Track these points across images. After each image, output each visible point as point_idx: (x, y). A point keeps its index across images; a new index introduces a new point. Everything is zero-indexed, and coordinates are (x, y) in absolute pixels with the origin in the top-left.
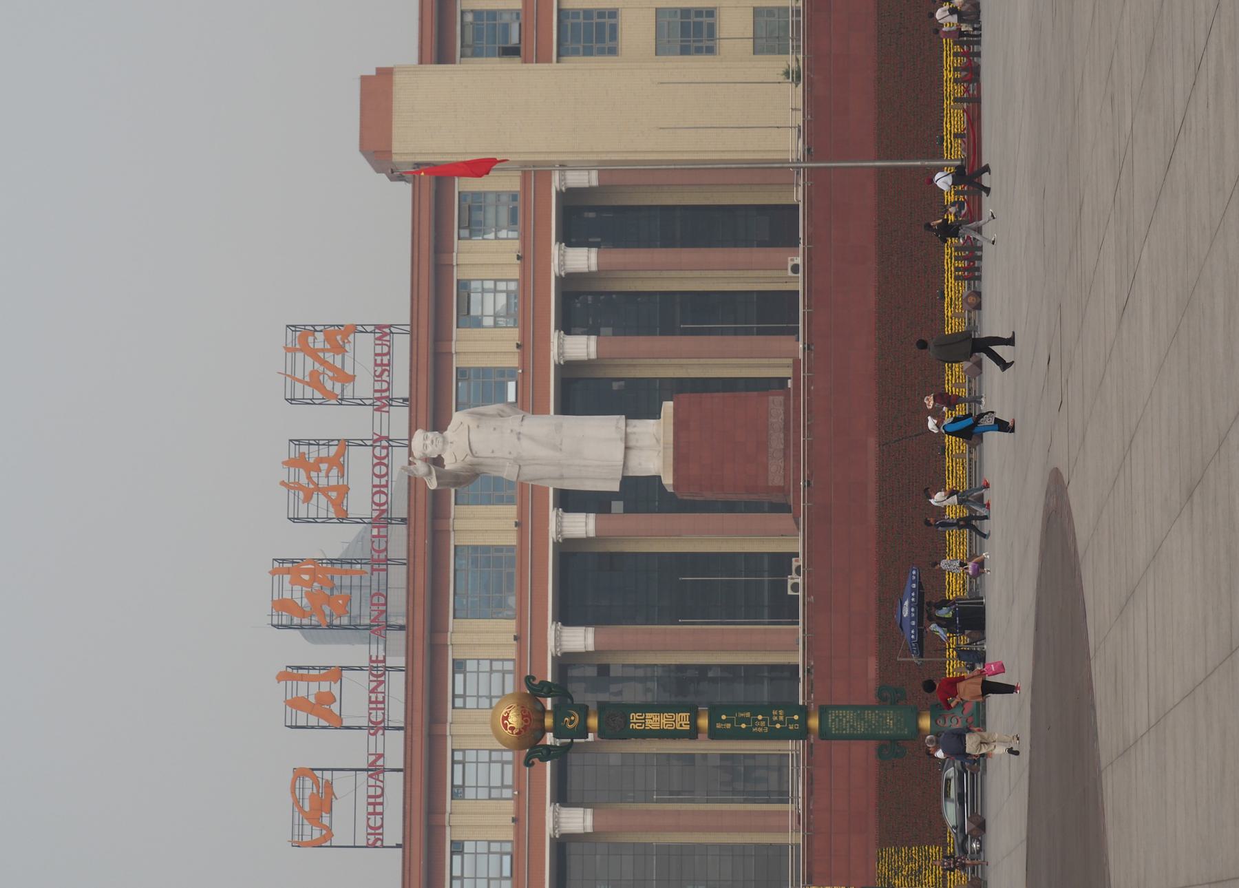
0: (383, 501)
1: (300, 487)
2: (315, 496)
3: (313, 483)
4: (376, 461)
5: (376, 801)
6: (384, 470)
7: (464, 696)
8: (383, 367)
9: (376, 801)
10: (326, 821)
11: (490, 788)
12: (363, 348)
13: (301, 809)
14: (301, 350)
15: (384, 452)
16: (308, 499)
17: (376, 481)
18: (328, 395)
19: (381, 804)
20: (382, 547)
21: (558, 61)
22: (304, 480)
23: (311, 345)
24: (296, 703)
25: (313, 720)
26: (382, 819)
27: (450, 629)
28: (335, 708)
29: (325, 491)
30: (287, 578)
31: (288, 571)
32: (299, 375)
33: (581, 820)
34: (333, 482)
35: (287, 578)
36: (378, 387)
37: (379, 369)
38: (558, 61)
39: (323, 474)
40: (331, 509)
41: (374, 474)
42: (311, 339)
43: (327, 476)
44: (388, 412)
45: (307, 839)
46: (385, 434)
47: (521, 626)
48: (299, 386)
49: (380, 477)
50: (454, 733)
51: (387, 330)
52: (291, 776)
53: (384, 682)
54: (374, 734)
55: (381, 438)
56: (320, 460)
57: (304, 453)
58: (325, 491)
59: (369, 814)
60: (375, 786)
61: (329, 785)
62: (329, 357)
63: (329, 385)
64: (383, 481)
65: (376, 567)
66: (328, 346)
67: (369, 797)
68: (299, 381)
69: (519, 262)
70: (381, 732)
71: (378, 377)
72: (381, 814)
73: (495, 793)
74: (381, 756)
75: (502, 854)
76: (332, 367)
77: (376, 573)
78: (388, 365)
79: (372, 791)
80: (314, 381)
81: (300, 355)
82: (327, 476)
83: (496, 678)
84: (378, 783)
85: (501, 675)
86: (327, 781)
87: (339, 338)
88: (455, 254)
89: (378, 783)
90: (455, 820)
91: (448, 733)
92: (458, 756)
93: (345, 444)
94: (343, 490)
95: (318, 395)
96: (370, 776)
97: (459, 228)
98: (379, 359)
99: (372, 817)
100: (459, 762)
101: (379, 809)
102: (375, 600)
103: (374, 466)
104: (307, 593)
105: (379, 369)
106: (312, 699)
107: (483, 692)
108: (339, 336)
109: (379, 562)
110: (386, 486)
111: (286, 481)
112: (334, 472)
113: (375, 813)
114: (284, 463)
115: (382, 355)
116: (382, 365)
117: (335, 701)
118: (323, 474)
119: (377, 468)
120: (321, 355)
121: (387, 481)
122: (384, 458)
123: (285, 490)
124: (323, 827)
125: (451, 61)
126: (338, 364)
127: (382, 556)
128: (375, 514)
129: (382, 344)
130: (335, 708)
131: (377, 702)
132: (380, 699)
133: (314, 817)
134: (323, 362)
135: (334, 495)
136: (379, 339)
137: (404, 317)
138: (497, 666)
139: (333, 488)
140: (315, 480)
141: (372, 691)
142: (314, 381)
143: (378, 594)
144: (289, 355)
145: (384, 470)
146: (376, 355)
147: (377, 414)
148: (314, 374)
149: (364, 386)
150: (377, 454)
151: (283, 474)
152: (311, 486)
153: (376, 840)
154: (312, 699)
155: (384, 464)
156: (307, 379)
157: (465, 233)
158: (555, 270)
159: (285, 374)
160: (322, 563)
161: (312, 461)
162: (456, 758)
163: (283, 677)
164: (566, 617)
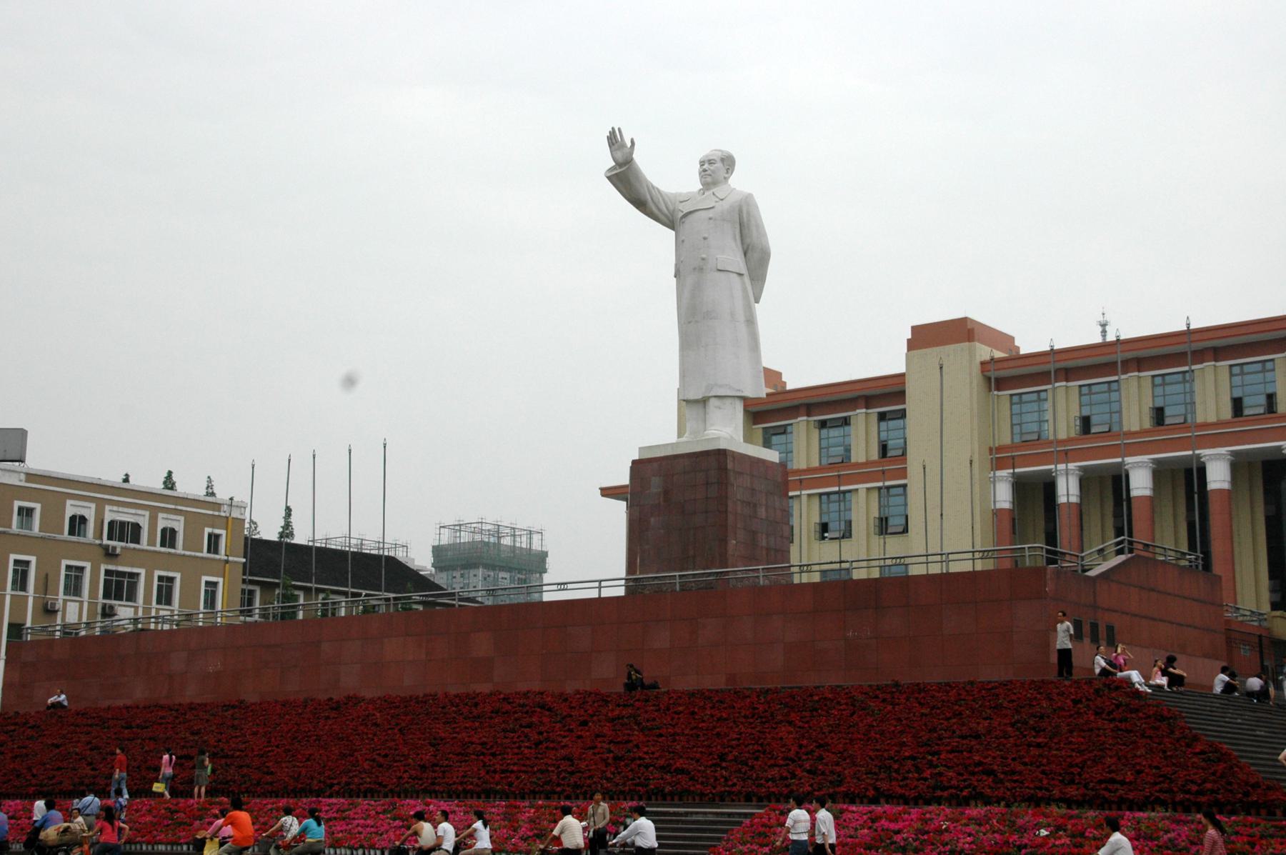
7: (1242, 373)
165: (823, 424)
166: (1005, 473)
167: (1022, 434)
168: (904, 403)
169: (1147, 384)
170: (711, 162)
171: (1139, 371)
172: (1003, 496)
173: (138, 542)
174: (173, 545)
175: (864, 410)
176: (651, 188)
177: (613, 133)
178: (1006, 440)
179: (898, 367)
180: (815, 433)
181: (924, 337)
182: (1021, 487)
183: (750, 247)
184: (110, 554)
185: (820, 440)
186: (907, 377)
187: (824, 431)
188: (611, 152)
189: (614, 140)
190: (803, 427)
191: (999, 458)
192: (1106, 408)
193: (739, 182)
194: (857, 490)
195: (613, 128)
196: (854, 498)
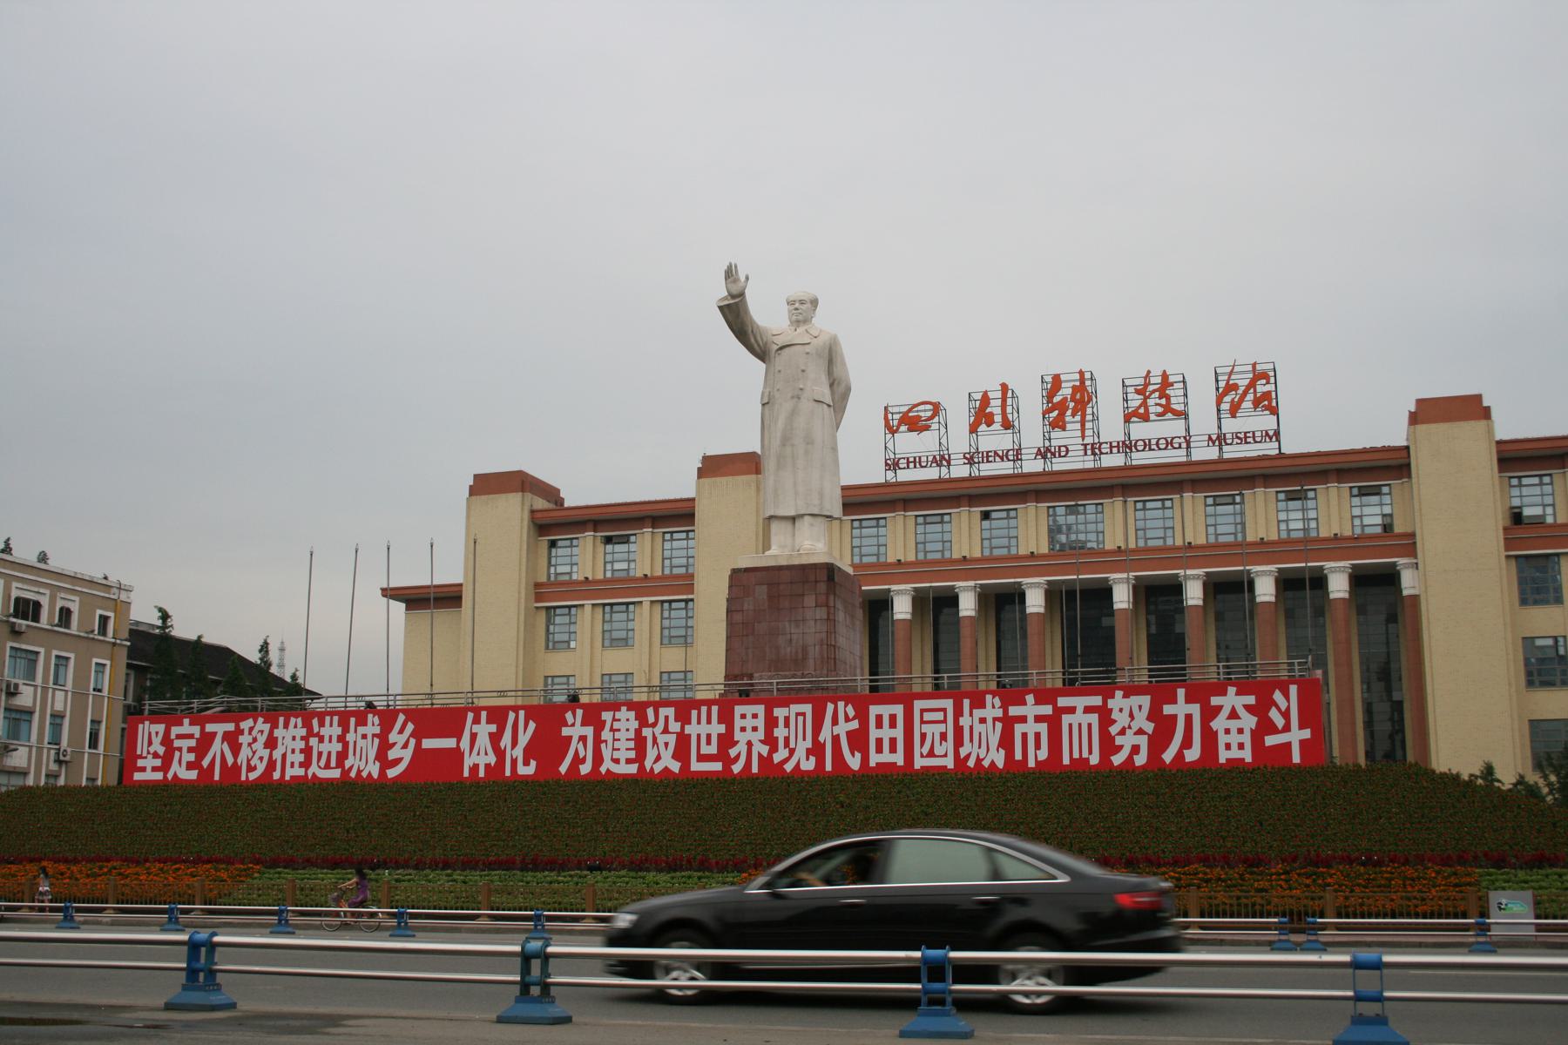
0: (1138, 448)
1: (1146, 385)
2: (1142, 397)
3: (1150, 395)
4: (1169, 440)
5: (916, 462)
6: (1162, 446)
8: (1244, 438)
9: (916, 462)
10: (903, 428)
11: (924, 543)
12: (1266, 422)
13: (910, 410)
14: (1254, 375)
16: (1138, 392)
17: (1154, 442)
18: (1219, 402)
19: (915, 467)
20: (1103, 451)
21: (1508, 557)
22: (1151, 388)
23: (1259, 382)
24: (985, 400)
26: (904, 468)
27: (1039, 505)
28: (983, 427)
29: (1144, 404)
30: (1078, 383)
32: (1233, 377)
33: (1034, 604)
34: (1152, 409)
35: (1078, 383)
36: (1228, 436)
37: (1242, 436)
38: (1508, 557)
39: (1158, 401)
40: (1130, 410)
41: (1159, 439)
42: (1264, 381)
43: (1157, 404)
44: (1208, 446)
45: (890, 416)
46: (1192, 445)
48: (1226, 378)
49: (1157, 444)
50: (963, 514)
51: (1274, 439)
52: (934, 401)
53: (1003, 460)
54: (965, 458)
55: (1188, 443)
56: (1168, 398)
57: (1173, 385)
58: (1144, 404)
59: (908, 459)
60: (927, 462)
61: (927, 428)
62: (1250, 397)
63: (1228, 399)
64: (1154, 447)
65: (1089, 447)
66: (1258, 395)
67: (920, 458)
68: (1229, 377)
69: (1258, 539)
70: (966, 461)
71: (1236, 435)
72: (908, 467)
73: (856, 550)
75: (878, 555)
77: (1082, 447)
78: (1246, 443)
79: (924, 459)
80: (1231, 388)
81: (1251, 376)
82: (1157, 404)
83: (1005, 542)
84: (929, 463)
85: (1007, 545)
86: (930, 427)
87: (1266, 403)
88: (1336, 484)
89: (929, 463)
90: (900, 520)
91: (962, 509)
92: (946, 518)
93: (1183, 415)
94: (1145, 418)
95: (1221, 390)
96: (935, 457)
97: (1359, 487)
98: (1251, 435)
99: (905, 461)
100: (942, 519)
101: (912, 465)
102: (1063, 449)
103: (1165, 439)
104: (1067, 398)
105: (1242, 436)
106: (988, 410)
107: (995, 533)
108: (1266, 402)
109: (1093, 449)
110: (1150, 449)
111: (1151, 375)
112: (1160, 410)
113: (908, 462)
114: (1165, 371)
115: (1254, 437)
116: (1246, 437)
117: (988, 426)
118: (1158, 401)
119: (1164, 441)
120: (1252, 391)
121: (1154, 450)
122: (1172, 446)
123: (1144, 374)
124: (898, 427)
125: (1501, 470)
126: (1244, 405)
127: (1097, 451)
129: (1262, 436)
130: (983, 427)
131: (988, 456)
132: (990, 459)
133: (902, 421)
134: (1245, 393)
135: (1142, 411)
136: (1267, 434)
137: (1286, 450)
138: (1013, 542)
140: (1153, 396)
141: (995, 453)
142: (1231, 388)
143: (1067, 451)
144: (1250, 368)
145: (1162, 446)
146: (1254, 433)
147: (1206, 438)
148: (1235, 387)
149: (1230, 426)
150: (1176, 440)
152: (1147, 394)
153: (893, 465)
154: (988, 410)
155: (1167, 446)
156: (1231, 382)
157: (1355, 491)
158: (1328, 565)
159: (1234, 366)
160: (1093, 408)
161: (1167, 392)
162: (945, 516)
163: (1004, 388)
164: (1052, 593)
165: (608, 540)
168: (693, 525)
169: (911, 522)
170: (802, 302)
171: (905, 511)
175: (650, 530)
176: (751, 318)
177: (730, 267)
179: (690, 493)
180: (601, 548)
183: (836, 382)
185: (605, 553)
186: (696, 502)
187: (609, 547)
188: (726, 284)
189: (730, 274)
190: (590, 541)
192: (874, 541)
193: (824, 322)
195: (731, 264)
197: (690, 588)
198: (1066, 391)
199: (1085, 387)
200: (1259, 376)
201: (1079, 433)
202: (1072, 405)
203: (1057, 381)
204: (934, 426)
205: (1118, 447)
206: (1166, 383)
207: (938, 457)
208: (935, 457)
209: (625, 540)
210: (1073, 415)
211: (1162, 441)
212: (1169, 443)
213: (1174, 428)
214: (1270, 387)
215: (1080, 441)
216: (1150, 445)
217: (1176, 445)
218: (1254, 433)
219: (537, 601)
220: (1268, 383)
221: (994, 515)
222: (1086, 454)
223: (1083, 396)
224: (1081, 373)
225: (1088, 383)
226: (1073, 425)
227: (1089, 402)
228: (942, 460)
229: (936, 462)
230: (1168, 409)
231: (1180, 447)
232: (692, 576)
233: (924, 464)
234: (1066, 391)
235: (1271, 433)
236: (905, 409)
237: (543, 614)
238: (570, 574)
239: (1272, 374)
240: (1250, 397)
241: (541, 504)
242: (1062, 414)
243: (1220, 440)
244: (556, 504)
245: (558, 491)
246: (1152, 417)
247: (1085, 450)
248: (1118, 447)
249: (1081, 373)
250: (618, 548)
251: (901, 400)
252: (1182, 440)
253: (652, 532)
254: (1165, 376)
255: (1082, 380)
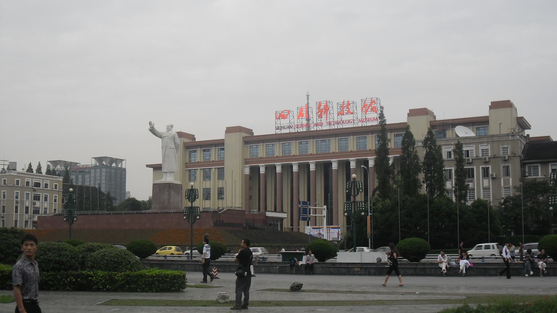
1: (343, 104)
15: (351, 122)
17: (345, 121)
22: (345, 105)
24: (302, 109)
25: (298, 113)
30: (325, 104)
31: (327, 104)
34: (345, 112)
35: (325, 104)
39: (346, 109)
41: (346, 120)
42: (374, 103)
47: (314, 155)
49: (346, 122)
56: (349, 108)
61: (287, 118)
62: (370, 108)
63: (364, 108)
64: (345, 123)
65: (328, 123)
74: (292, 127)
76: (368, 109)
77: (326, 123)
79: (285, 127)
80: (365, 106)
81: (370, 101)
82: (346, 110)
96: (288, 126)
103: (348, 120)
106: (302, 112)
110: (344, 123)
112: (347, 112)
115: (371, 120)
116: (369, 120)
118: (346, 109)
123: (343, 102)
128: (338, 122)
139: (343, 112)
148: (367, 105)
151: (346, 101)
153: (277, 128)
164: (317, 164)
165: (204, 151)
166: (248, 165)
167: (252, 156)
172: (247, 171)
173: (40, 187)
174: (47, 188)
178: (249, 157)
181: (229, 130)
182: (252, 168)
184: (35, 190)
191: (246, 162)
194: (212, 168)
196: (211, 169)
197: (223, 164)
198: (322, 107)
199: (327, 105)
200: (373, 102)
201: (325, 119)
202: (324, 111)
203: (320, 104)
204: (288, 117)
205: (336, 123)
206: (349, 104)
207: (289, 126)
208: (288, 126)
209: (209, 150)
210: (324, 114)
211: (347, 121)
212: (349, 121)
213: (349, 117)
214: (374, 105)
215: (326, 121)
216: (344, 122)
217: (351, 122)
218: (371, 118)
219: (186, 168)
220: (375, 104)
221: (302, 143)
222: (327, 125)
223: (327, 109)
224: (326, 101)
225: (328, 104)
226: (324, 116)
227: (328, 110)
228: (289, 127)
229: (289, 127)
230: (349, 112)
231: (352, 123)
232: (223, 161)
233: (285, 128)
234: (322, 107)
235: (375, 118)
236: (280, 112)
237: (188, 172)
238: (195, 160)
239: (376, 101)
240: (370, 108)
241: (186, 140)
242: (321, 114)
243: (362, 121)
244: (193, 140)
245: (194, 136)
246: (345, 114)
247: (327, 124)
248: (336, 123)
249: (326, 101)
250: (207, 153)
251: (280, 109)
252: (352, 120)
253: (215, 148)
254: (348, 102)
255: (327, 103)
